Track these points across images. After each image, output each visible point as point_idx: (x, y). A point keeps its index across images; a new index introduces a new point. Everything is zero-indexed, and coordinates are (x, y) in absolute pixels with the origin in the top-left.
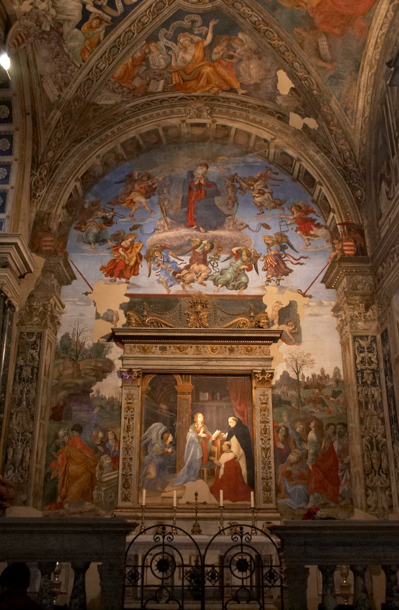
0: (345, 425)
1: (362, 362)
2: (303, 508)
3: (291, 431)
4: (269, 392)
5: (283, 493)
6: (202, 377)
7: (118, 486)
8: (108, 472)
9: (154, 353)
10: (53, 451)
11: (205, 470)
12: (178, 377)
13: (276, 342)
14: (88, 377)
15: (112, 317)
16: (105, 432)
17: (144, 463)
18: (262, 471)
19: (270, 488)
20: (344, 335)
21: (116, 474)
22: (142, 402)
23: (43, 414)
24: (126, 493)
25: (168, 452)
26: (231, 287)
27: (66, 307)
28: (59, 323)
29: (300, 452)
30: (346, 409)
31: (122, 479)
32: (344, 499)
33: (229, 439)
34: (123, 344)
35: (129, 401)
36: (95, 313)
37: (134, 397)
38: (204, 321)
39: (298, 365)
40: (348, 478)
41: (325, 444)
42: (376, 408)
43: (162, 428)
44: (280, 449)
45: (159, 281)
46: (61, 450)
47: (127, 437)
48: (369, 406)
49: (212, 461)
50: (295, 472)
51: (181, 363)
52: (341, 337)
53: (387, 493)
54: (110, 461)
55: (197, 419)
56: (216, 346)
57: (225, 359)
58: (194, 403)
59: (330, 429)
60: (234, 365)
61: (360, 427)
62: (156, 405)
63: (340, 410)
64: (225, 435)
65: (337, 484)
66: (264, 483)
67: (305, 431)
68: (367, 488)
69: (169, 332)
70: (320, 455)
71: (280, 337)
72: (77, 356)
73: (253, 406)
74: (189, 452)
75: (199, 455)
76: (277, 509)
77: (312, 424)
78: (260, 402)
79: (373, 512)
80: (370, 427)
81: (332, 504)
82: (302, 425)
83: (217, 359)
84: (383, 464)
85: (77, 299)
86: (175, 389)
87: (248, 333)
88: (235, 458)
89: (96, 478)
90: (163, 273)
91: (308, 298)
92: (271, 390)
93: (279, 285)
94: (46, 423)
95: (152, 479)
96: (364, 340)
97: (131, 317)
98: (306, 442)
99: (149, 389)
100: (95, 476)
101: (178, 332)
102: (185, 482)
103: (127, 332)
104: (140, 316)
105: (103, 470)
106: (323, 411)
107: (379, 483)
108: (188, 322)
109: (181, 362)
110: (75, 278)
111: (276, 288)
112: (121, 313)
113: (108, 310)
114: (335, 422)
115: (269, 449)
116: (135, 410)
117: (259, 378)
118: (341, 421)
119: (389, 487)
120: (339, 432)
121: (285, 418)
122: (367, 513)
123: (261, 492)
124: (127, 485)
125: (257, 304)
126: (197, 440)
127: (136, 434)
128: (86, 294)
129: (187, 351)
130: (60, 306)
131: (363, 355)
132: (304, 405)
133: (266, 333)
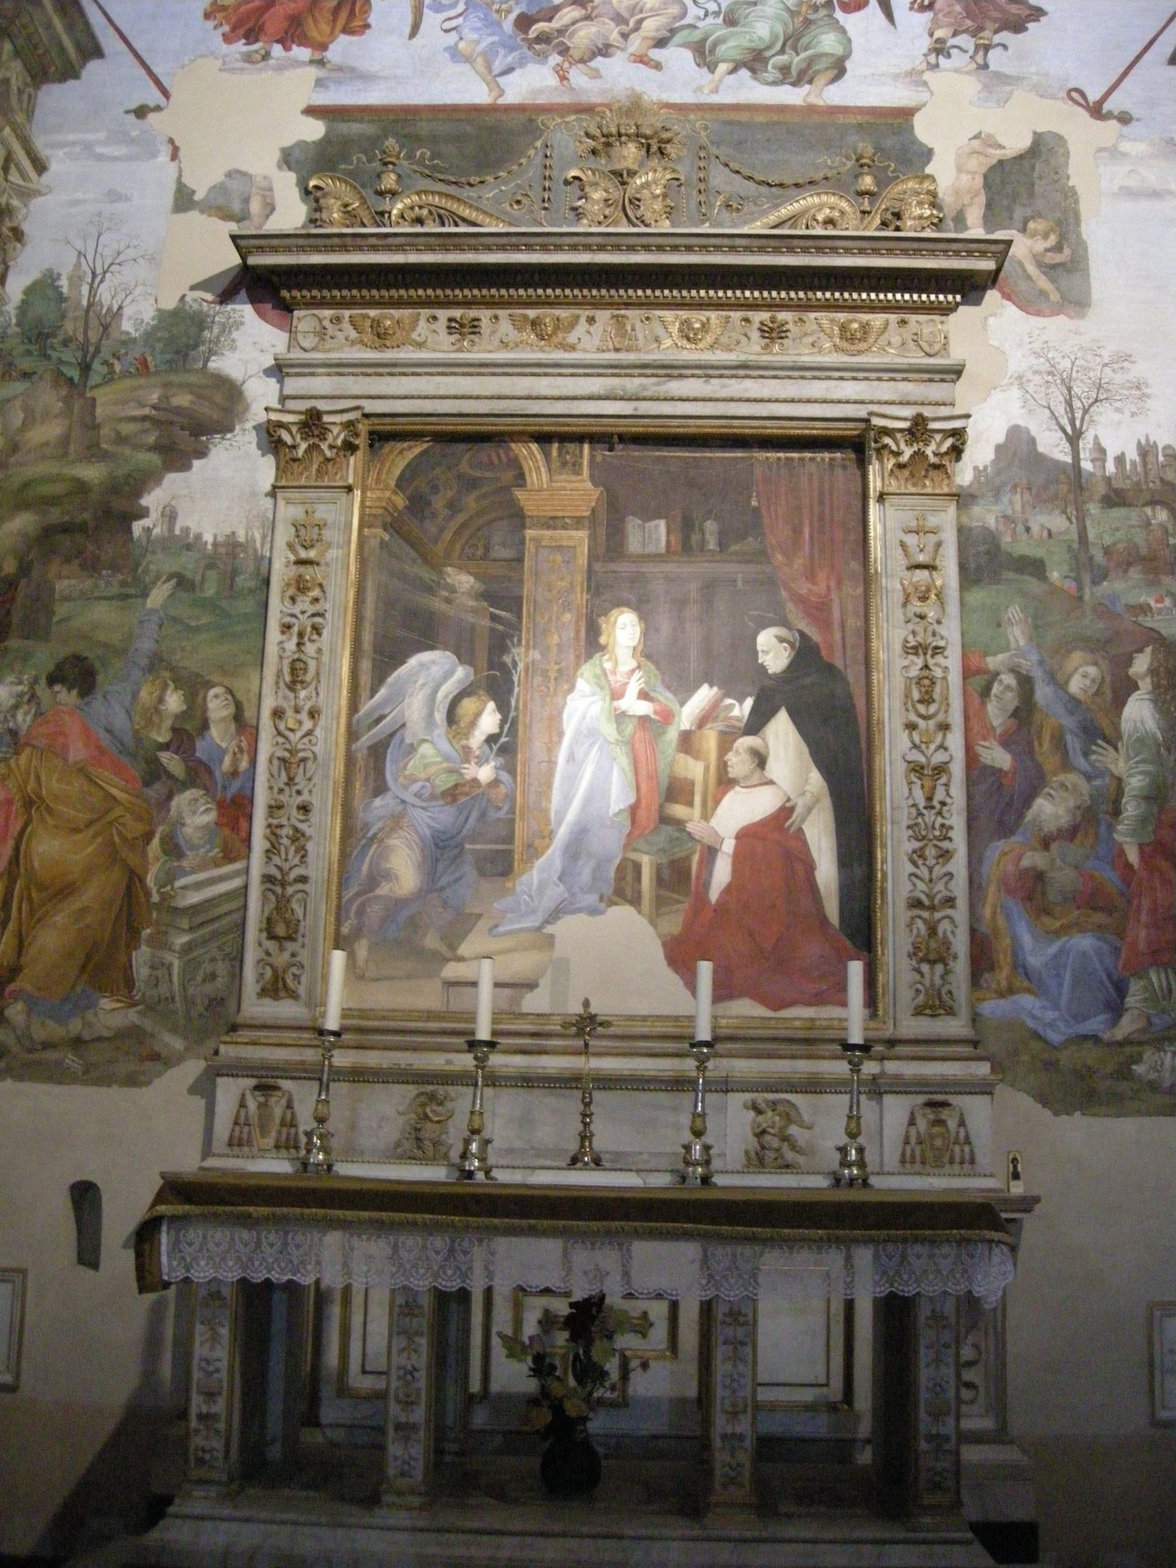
2: (1095, 1039)
3: (1043, 693)
4: (947, 518)
6: (636, 452)
7: (242, 925)
8: (203, 867)
9: (420, 345)
11: (646, 861)
12: (530, 454)
13: (978, 302)
14: (127, 451)
15: (246, 201)
17: (367, 826)
18: (910, 868)
19: (947, 944)
21: (236, 874)
22: (362, 560)
24: (281, 959)
25: (475, 781)
26: (772, 73)
27: (54, 167)
28: (18, 235)
29: (1084, 787)
31: (264, 899)
33: (757, 723)
34: (287, 308)
36: (172, 187)
38: (652, 208)
39: (1077, 404)
44: (997, 772)
45: (455, 54)
47: (290, 713)
49: (679, 824)
50: (1063, 877)
51: (543, 386)
54: (211, 817)
56: (702, 315)
57: (744, 369)
58: (597, 566)
60: (783, 395)
64: (742, 709)
66: (920, 924)
69: (488, 248)
71: (992, 279)
72: (86, 368)
73: (867, 580)
74: (572, 780)
75: (619, 796)
76: (975, 1044)
77: (1141, 664)
78: (904, 562)
82: (1096, 664)
83: (706, 370)
85: (101, 136)
87: (848, 251)
88: (785, 812)
89: (148, 894)
90: (474, 20)
91: (1114, 123)
92: (952, 509)
93: (985, 66)
95: (399, 904)
97: (324, 196)
98: (1113, 741)
99: (400, 501)
100: (142, 881)
101: (530, 248)
102: (555, 915)
103: (302, 249)
104: (368, 193)
105: (180, 855)
108: (578, 213)
109: (545, 381)
110: (97, 52)
111: (972, 79)
112: (286, 186)
113: (229, 175)
115: (941, 770)
116: (331, 590)
117: (897, 454)
121: (1017, 635)
123: (905, 964)
125: (889, 143)
126: (609, 730)
128: (141, 112)
129: (572, 338)
130: (26, 164)
133: (933, 253)
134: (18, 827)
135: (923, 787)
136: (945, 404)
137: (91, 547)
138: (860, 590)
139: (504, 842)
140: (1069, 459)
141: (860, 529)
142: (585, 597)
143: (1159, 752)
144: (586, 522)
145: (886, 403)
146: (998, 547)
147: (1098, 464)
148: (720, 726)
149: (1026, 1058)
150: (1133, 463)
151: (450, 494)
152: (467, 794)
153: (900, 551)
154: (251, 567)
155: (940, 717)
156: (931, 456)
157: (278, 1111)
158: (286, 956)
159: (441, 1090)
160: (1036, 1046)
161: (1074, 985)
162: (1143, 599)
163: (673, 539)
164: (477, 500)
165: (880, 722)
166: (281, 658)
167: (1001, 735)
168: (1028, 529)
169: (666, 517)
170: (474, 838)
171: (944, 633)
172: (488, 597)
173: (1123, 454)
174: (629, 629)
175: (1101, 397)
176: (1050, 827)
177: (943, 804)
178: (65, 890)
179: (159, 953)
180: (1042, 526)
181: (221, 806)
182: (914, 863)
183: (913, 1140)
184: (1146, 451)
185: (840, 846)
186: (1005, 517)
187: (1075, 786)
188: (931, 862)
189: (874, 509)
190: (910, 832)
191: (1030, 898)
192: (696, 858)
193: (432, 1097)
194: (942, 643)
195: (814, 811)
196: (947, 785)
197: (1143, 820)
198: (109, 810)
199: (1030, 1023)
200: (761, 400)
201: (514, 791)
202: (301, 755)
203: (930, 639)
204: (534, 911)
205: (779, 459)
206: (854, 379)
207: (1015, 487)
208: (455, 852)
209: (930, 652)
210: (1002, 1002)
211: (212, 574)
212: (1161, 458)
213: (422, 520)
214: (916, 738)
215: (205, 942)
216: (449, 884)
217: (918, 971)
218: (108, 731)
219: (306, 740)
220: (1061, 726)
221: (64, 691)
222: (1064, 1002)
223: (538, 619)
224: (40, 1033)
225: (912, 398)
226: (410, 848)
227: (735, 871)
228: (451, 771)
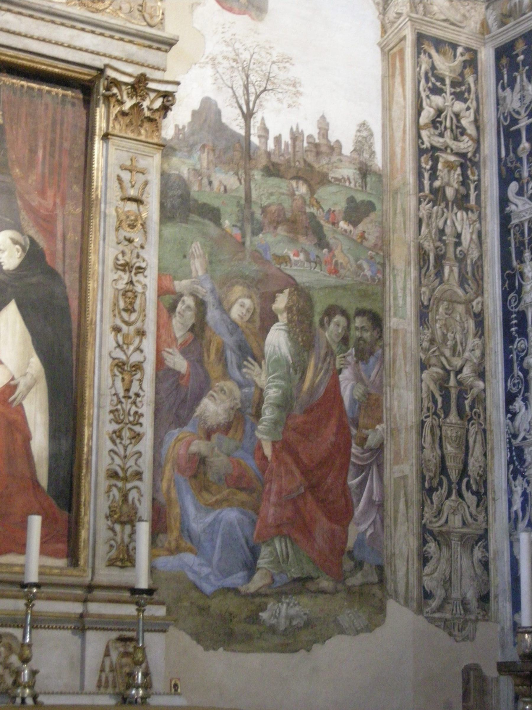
1: (435, 123)
2: (235, 590)
5: (175, 534)
18: (109, 445)
20: (393, 23)
29: (237, 392)
30: (383, 265)
39: (251, 89)
40: (376, 497)
41: (315, 375)
42: (462, 281)
44: (176, 374)
52: (384, 30)
53: (478, 553)
59: (332, 326)
61: (418, 333)
63: (365, 266)
66: (115, 491)
67: (258, 323)
70: (297, 412)
78: (119, 194)
79: (437, 615)
80: (444, 336)
81: (325, 583)
82: (250, 297)
84: (471, 461)
92: (158, 157)
96: (444, 54)
98: (258, 358)
106: (318, 262)
107: (456, 521)
115: (138, 367)
117: (121, 103)
118: (366, 305)
119: (484, 536)
120: (360, 339)
122: (420, 617)
123: (103, 524)
131: (438, 100)
132: (261, 230)
135: (123, 379)
136: (158, 69)
138: (79, 210)
140: (242, 132)
141: (83, 158)
143: (288, 372)
145: (115, 58)
146: (189, 194)
147: (263, 140)
149: (186, 604)
150: (287, 145)
153: (117, 184)
155: (139, 324)
156: (146, 110)
165: (93, 323)
167: (181, 345)
168: (210, 183)
171: (146, 256)
173: (280, 135)
175: (269, 87)
176: (212, 421)
180: (221, 182)
182: (114, 442)
184: (296, 136)
186: (195, 170)
187: (231, 391)
188: (126, 442)
189: (98, 145)
190: (111, 416)
191: (195, 476)
194: (143, 265)
195: (33, 390)
196: (140, 381)
197: (276, 423)
200: (19, 34)
203: (135, 260)
205: (22, 86)
206: (93, 32)
207: (204, 147)
209: (134, 271)
210: (171, 558)
212: (305, 144)
217: (112, 529)
220: (224, 343)
225: (136, 59)
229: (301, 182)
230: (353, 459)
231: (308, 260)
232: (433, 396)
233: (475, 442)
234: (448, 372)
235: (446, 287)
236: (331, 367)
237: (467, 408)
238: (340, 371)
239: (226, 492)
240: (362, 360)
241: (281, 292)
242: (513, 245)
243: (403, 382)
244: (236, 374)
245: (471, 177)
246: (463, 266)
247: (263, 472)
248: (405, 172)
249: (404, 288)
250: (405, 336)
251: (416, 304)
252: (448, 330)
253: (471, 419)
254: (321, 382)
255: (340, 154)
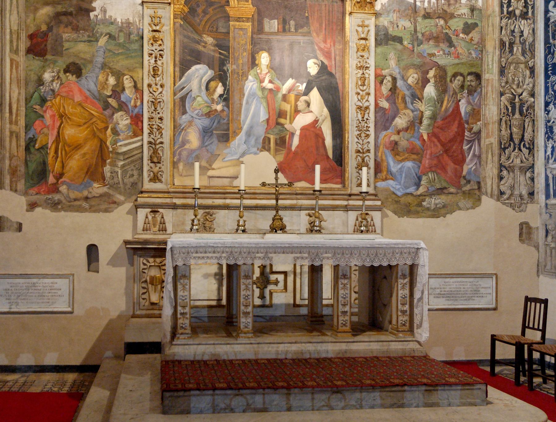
0: (478, 77)
2: (411, 194)
3: (400, 83)
4: (372, 22)
5: (385, 173)
10: (36, 104)
11: (272, 137)
16: (119, 76)
17: (180, 125)
18: (356, 140)
22: (175, 31)
23: (15, 44)
24: (156, 170)
25: (216, 110)
29: (411, 114)
30: (482, 51)
31: (149, 150)
32: (469, 182)
33: (307, 92)
35: (155, 28)
37: (163, 21)
40: (477, 153)
41: (448, 104)
42: (524, 53)
43: (207, 72)
44: (384, 109)
46: (49, 104)
47: (154, 86)
48: (515, 49)
49: (282, 125)
50: (404, 143)
53: (528, 174)
54: (128, 121)
55: (260, 60)
58: (255, 36)
59: (456, 81)
61: (499, 80)
62: (197, 37)
63: (473, 52)
64: (302, 87)
65: (461, 161)
66: (359, 158)
67: (420, 84)
68: (501, 167)
70: (439, 120)
73: (345, 43)
74: (248, 110)
75: (263, 116)
76: (376, 195)
77: (431, 74)
78: (357, 37)
80: (513, 80)
81: (452, 190)
82: (417, 73)
84: (526, 134)
86: (226, 12)
88: (316, 121)
92: (373, 19)
94: (21, 58)
95: (193, 151)
102: (243, 154)
105: (119, 135)
106: (449, 54)
107: (518, 161)
114: (465, 71)
115: (367, 108)
116: (165, 41)
118: (473, 70)
119: (532, 167)
120: (469, 86)
121: (393, 63)
122: (499, 202)
124: (155, 159)
126: (260, 93)
127: (168, 81)
132: (422, 43)
134: (58, 125)
137: (75, 22)
139: (226, 131)
142: (251, 47)
144: (250, 20)
147: (422, 3)
148: (295, 92)
149: (390, 200)
150: (434, 3)
151: (204, 7)
152: (213, 114)
154: (136, 32)
155: (367, 91)
157: (159, 219)
158: (158, 168)
159: (211, 211)
160: (394, 196)
161: (405, 178)
162: (433, 52)
163: (279, 27)
164: (213, 10)
166: (149, 66)
168: (398, 26)
169: (277, 19)
170: (216, 129)
171: (369, 62)
172: (219, 46)
174: (265, 59)
176: (400, 127)
177: (367, 119)
178: (78, 147)
179: (113, 168)
181: (131, 117)
183: (357, 225)
185: (333, 133)
186: (391, 22)
187: (408, 114)
188: (363, 138)
189: (347, 17)
191: (393, 150)
192: (288, 136)
193: (208, 213)
194: (368, 66)
195: (325, 121)
197: (429, 125)
198: (91, 119)
199: (392, 189)
201: (229, 114)
202: (158, 100)
204: (236, 153)
207: (394, 11)
208: (210, 134)
210: (383, 182)
211: (122, 34)
213: (194, 16)
214: (360, 98)
215: (129, 164)
216: (209, 145)
218: (89, 91)
219: (160, 95)
220: (405, 94)
221: (71, 76)
222: (402, 182)
223: (235, 54)
224: (72, 195)
226: (195, 132)
227: (300, 141)
228: (208, 107)
229: (441, 19)
230: (466, 138)
231: (444, 54)
232: (507, 107)
233: (528, 126)
234: (515, 96)
235: (515, 57)
236: (455, 99)
237: (525, 111)
238: (460, 100)
239: (407, 155)
240: (471, 95)
241: (431, 69)
242: (551, 32)
243: (491, 103)
244: (410, 106)
245: (530, 3)
246: (524, 46)
247: (423, 146)
248: (494, 6)
249: (493, 60)
250: (492, 81)
251: (499, 66)
252: (515, 77)
253: (527, 115)
254: (450, 106)
255: (460, 3)
